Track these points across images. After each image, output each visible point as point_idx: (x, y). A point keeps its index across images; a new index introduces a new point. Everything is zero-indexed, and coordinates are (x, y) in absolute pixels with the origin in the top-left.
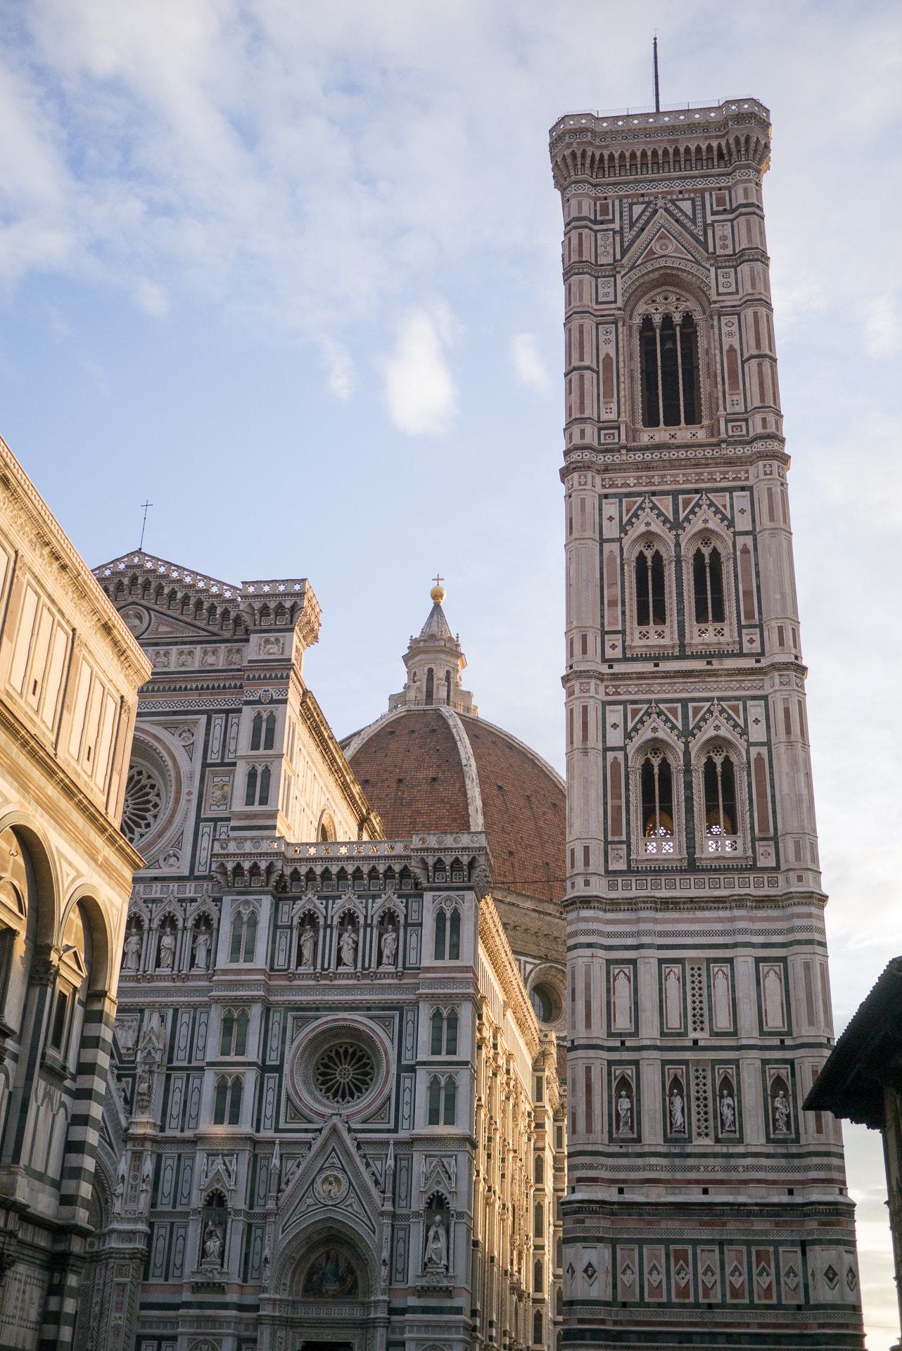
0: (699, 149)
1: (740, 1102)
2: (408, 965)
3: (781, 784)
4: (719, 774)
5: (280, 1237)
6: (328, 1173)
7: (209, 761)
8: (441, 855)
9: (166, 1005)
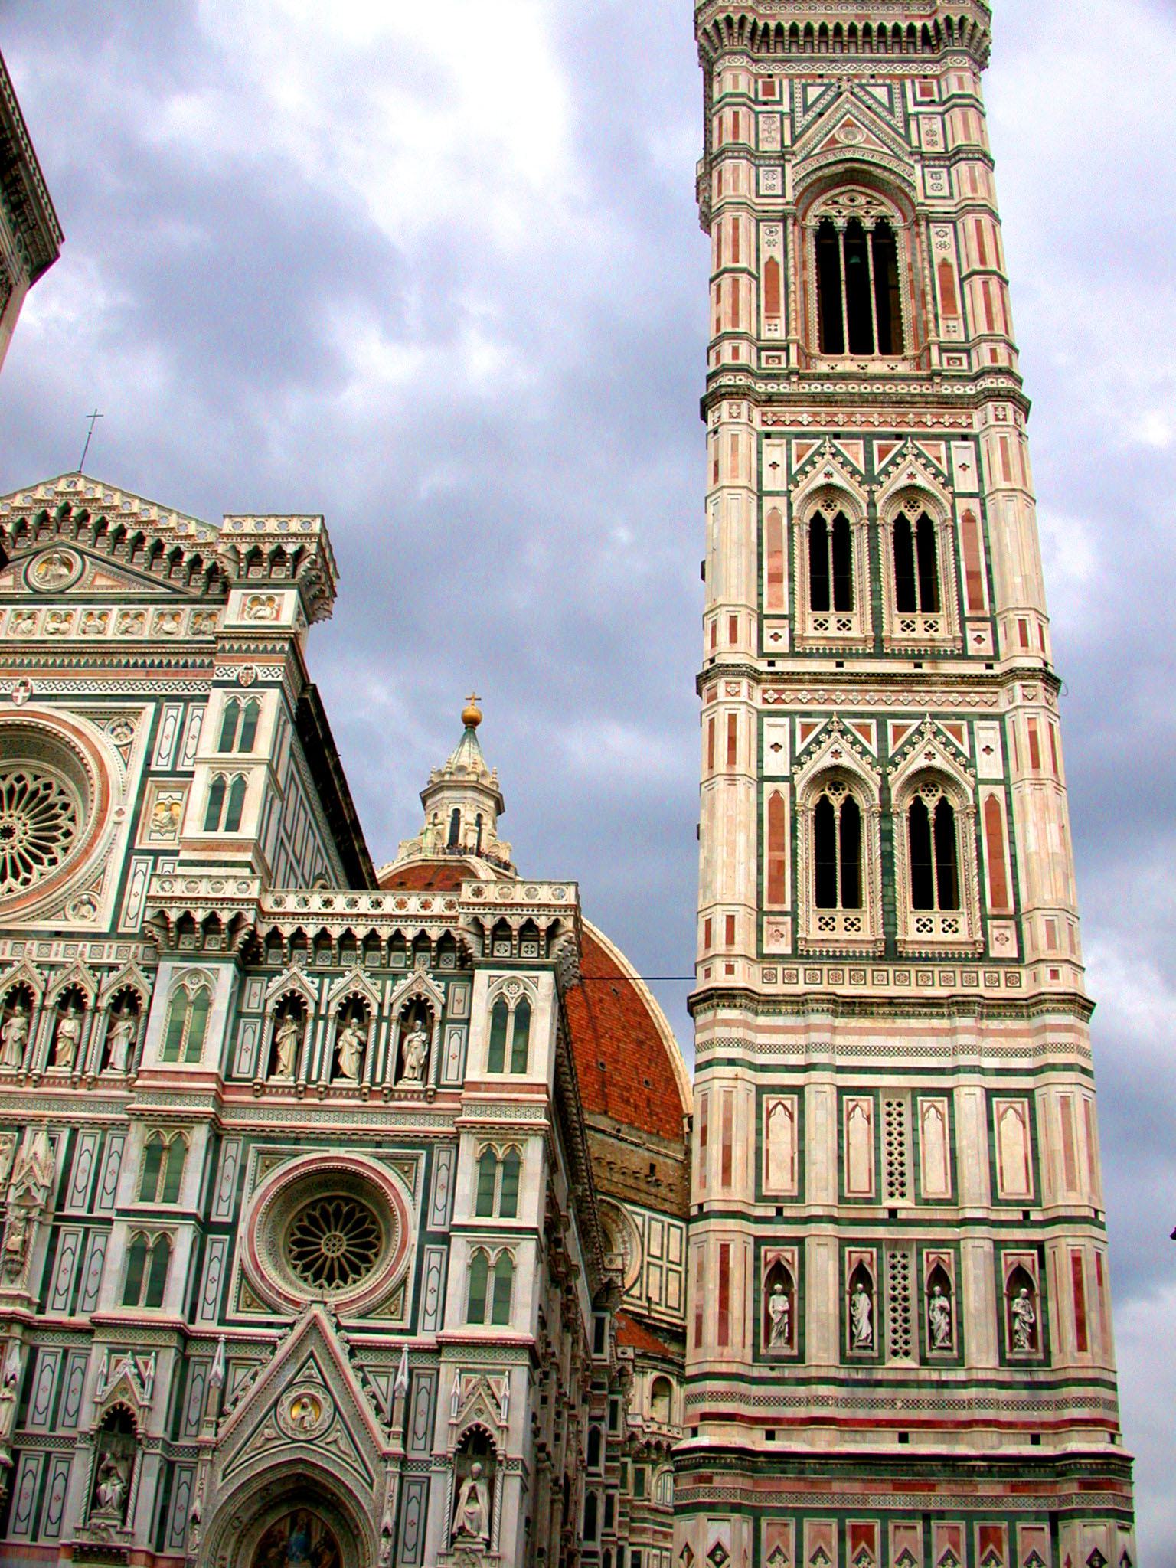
0: (897, 28)
1: (959, 1303)
2: (444, 1082)
3: (1025, 839)
4: (932, 822)
5: (220, 1484)
6: (302, 1391)
7: (153, 768)
8: (505, 913)
9: (59, 1122)
